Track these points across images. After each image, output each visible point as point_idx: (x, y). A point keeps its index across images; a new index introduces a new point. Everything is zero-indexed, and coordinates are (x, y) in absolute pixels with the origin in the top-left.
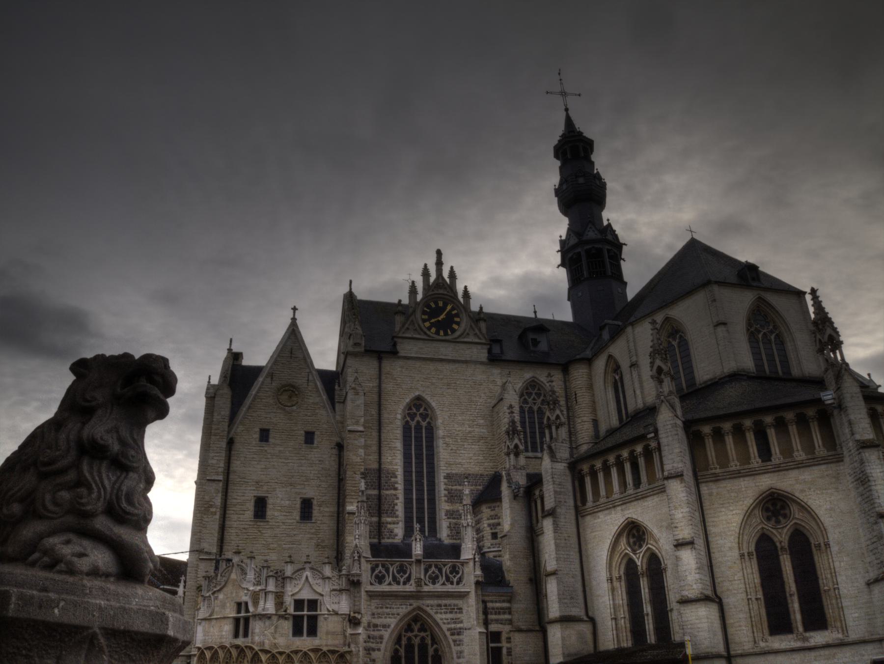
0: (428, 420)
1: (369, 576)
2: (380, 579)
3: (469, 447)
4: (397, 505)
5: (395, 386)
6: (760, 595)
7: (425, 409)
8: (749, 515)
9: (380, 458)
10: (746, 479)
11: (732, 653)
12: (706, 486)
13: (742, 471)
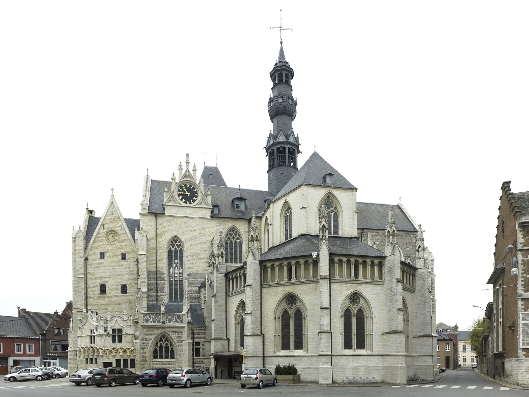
0: (180, 247)
1: (143, 319)
2: (147, 321)
3: (199, 260)
4: (165, 287)
5: (164, 231)
6: (280, 334)
7: (179, 242)
8: (280, 302)
9: (157, 266)
10: (281, 287)
11: (266, 355)
12: (266, 289)
13: (280, 284)
